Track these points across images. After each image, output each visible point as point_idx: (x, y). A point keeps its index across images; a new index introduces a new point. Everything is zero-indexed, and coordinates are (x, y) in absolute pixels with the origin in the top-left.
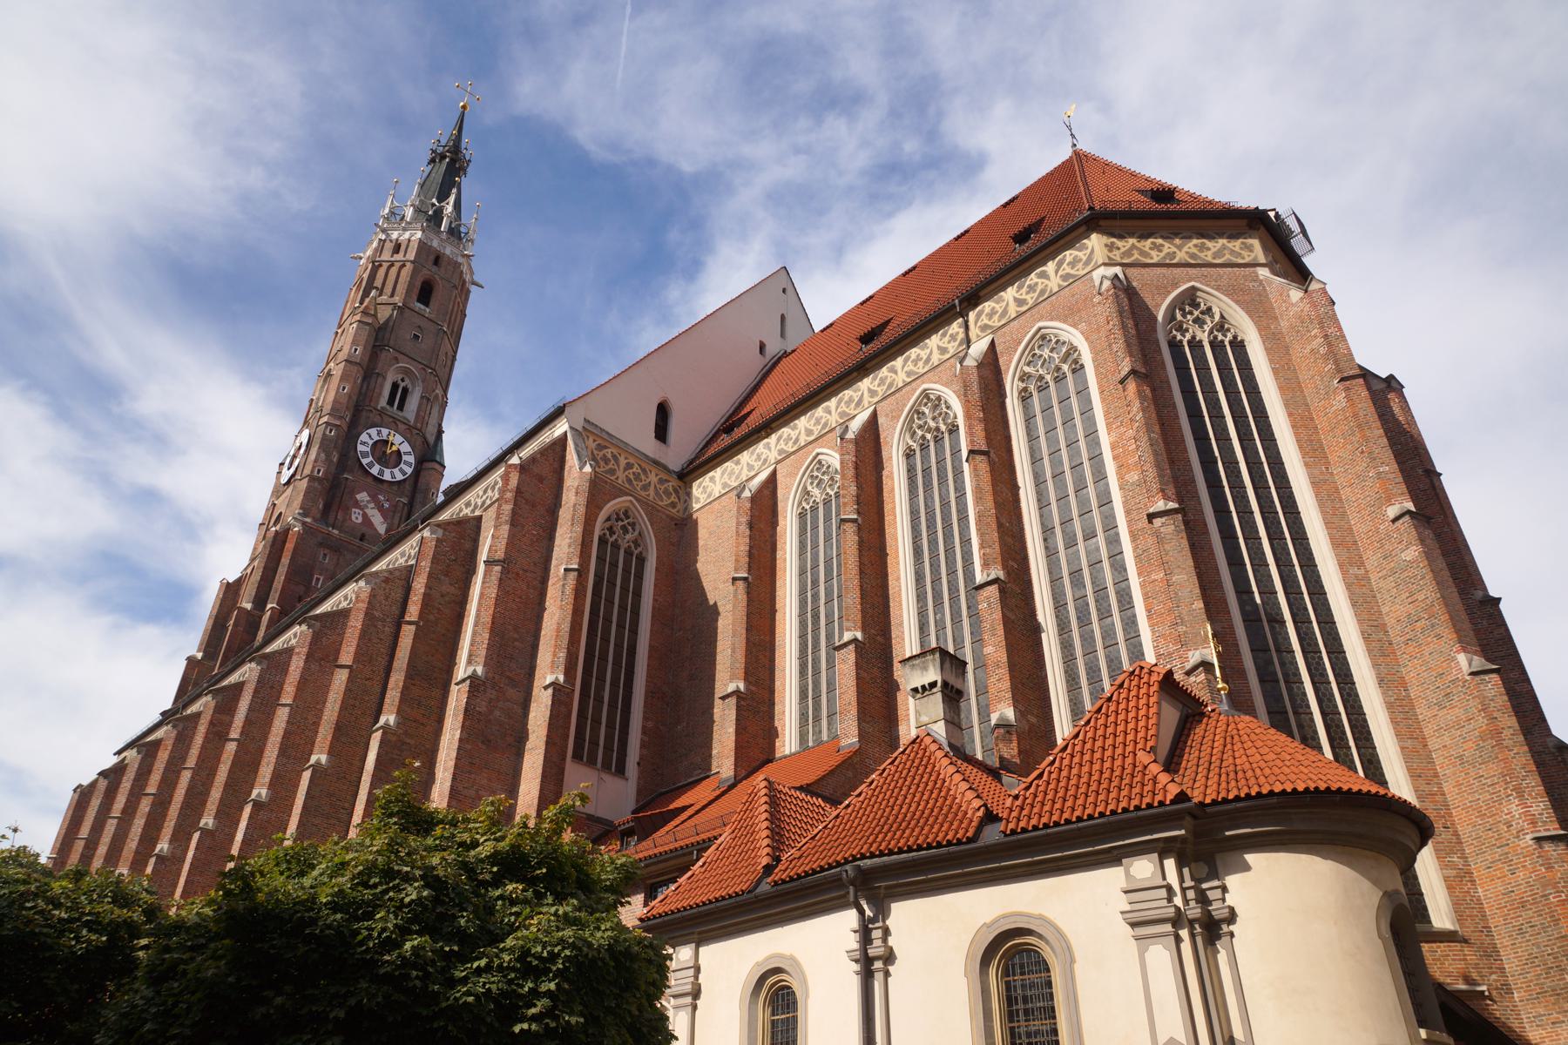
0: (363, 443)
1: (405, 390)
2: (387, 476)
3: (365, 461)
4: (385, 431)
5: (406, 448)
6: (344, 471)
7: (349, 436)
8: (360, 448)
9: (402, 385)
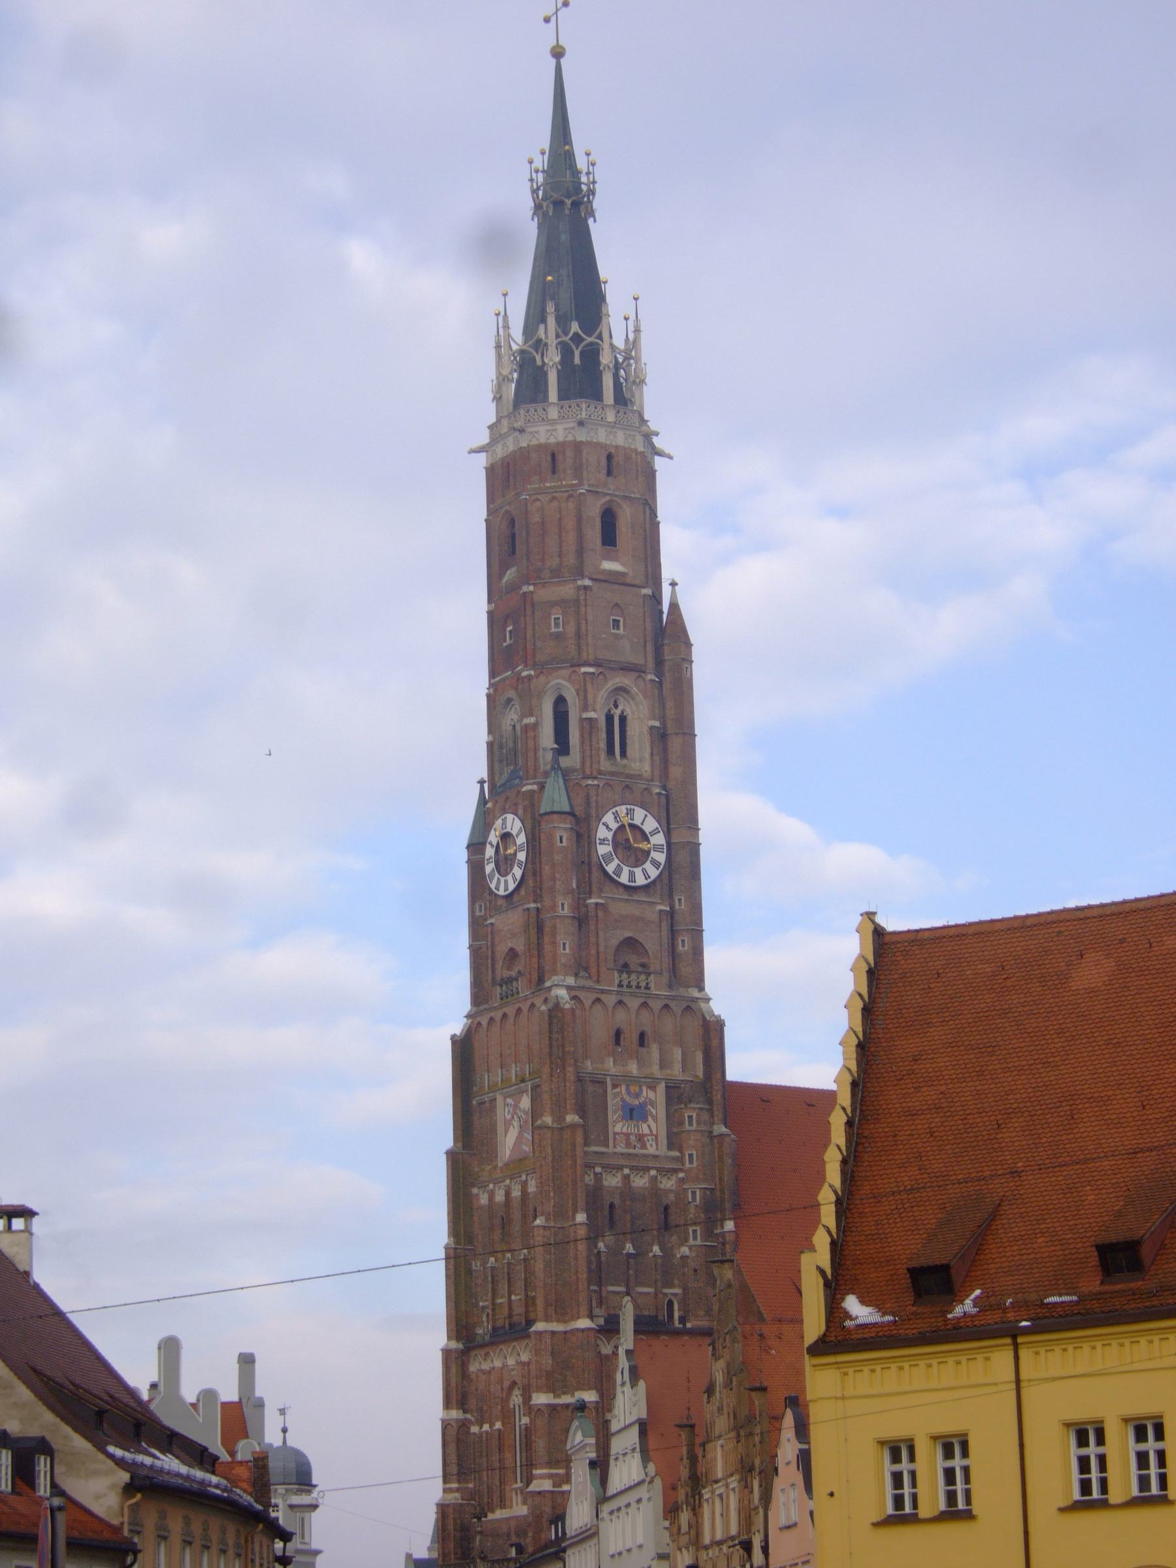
0: (603, 841)
1: (623, 719)
2: (640, 881)
3: (610, 869)
4: (622, 810)
5: (650, 825)
6: (590, 894)
7: (583, 828)
8: (603, 850)
9: (617, 713)
